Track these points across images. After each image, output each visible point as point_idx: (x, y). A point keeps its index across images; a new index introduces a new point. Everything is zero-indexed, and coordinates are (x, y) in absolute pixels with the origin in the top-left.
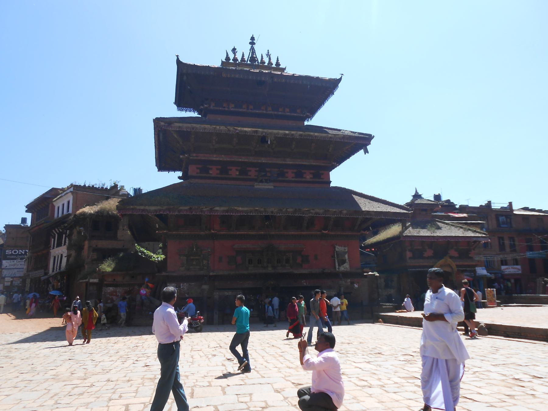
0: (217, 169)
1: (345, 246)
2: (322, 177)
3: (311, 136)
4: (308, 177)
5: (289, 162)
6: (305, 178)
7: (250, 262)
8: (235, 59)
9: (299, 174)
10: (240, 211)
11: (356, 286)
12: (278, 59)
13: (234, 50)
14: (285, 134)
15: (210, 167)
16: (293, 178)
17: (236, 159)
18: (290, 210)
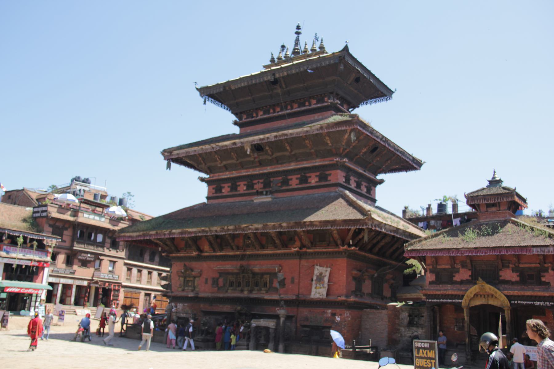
0: (229, 187)
1: (327, 267)
2: (329, 178)
3: (286, 135)
4: (313, 181)
5: (293, 166)
6: (310, 183)
7: (231, 284)
8: (279, 59)
9: (304, 180)
10: (190, 233)
11: (338, 319)
12: (322, 41)
13: (283, 47)
14: (261, 140)
15: (223, 185)
16: (297, 185)
17: (244, 173)
18: (231, 227)
